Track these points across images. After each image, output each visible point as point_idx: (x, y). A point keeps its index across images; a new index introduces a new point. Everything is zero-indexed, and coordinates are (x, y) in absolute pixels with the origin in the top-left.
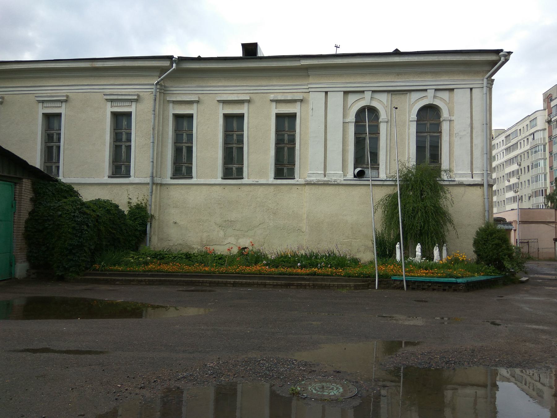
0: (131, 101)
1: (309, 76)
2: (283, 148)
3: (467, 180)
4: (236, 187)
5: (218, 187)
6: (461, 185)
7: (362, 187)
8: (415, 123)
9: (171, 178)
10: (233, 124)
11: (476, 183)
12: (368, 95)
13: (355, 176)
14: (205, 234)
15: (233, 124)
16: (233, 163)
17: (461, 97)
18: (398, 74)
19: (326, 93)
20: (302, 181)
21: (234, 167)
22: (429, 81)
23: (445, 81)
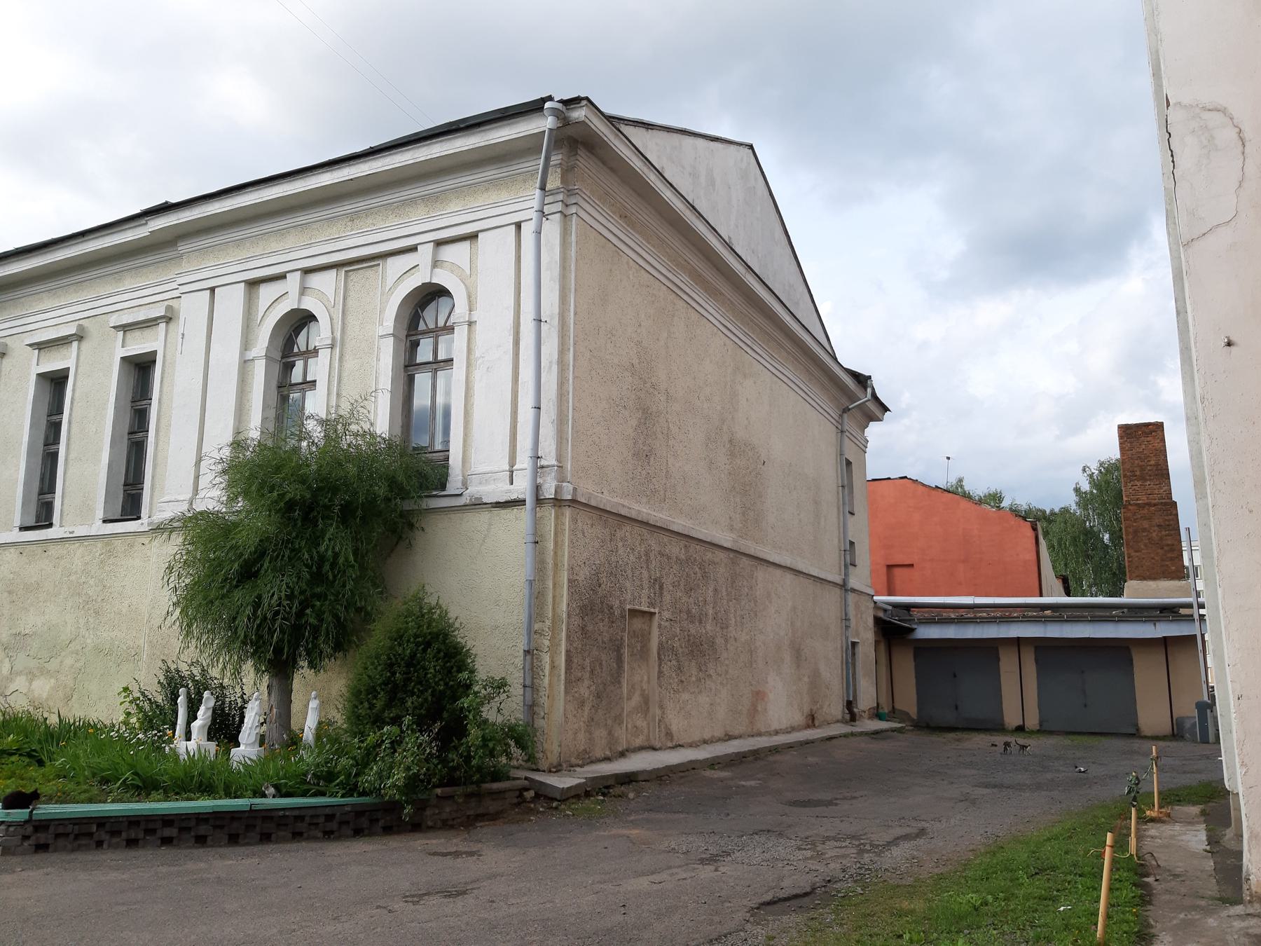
1: (181, 256)
4: (38, 549)
6: (478, 505)
12: (294, 281)
17: (496, 250)
18: (353, 217)
19: (212, 290)
22: (419, 223)
23: (453, 215)
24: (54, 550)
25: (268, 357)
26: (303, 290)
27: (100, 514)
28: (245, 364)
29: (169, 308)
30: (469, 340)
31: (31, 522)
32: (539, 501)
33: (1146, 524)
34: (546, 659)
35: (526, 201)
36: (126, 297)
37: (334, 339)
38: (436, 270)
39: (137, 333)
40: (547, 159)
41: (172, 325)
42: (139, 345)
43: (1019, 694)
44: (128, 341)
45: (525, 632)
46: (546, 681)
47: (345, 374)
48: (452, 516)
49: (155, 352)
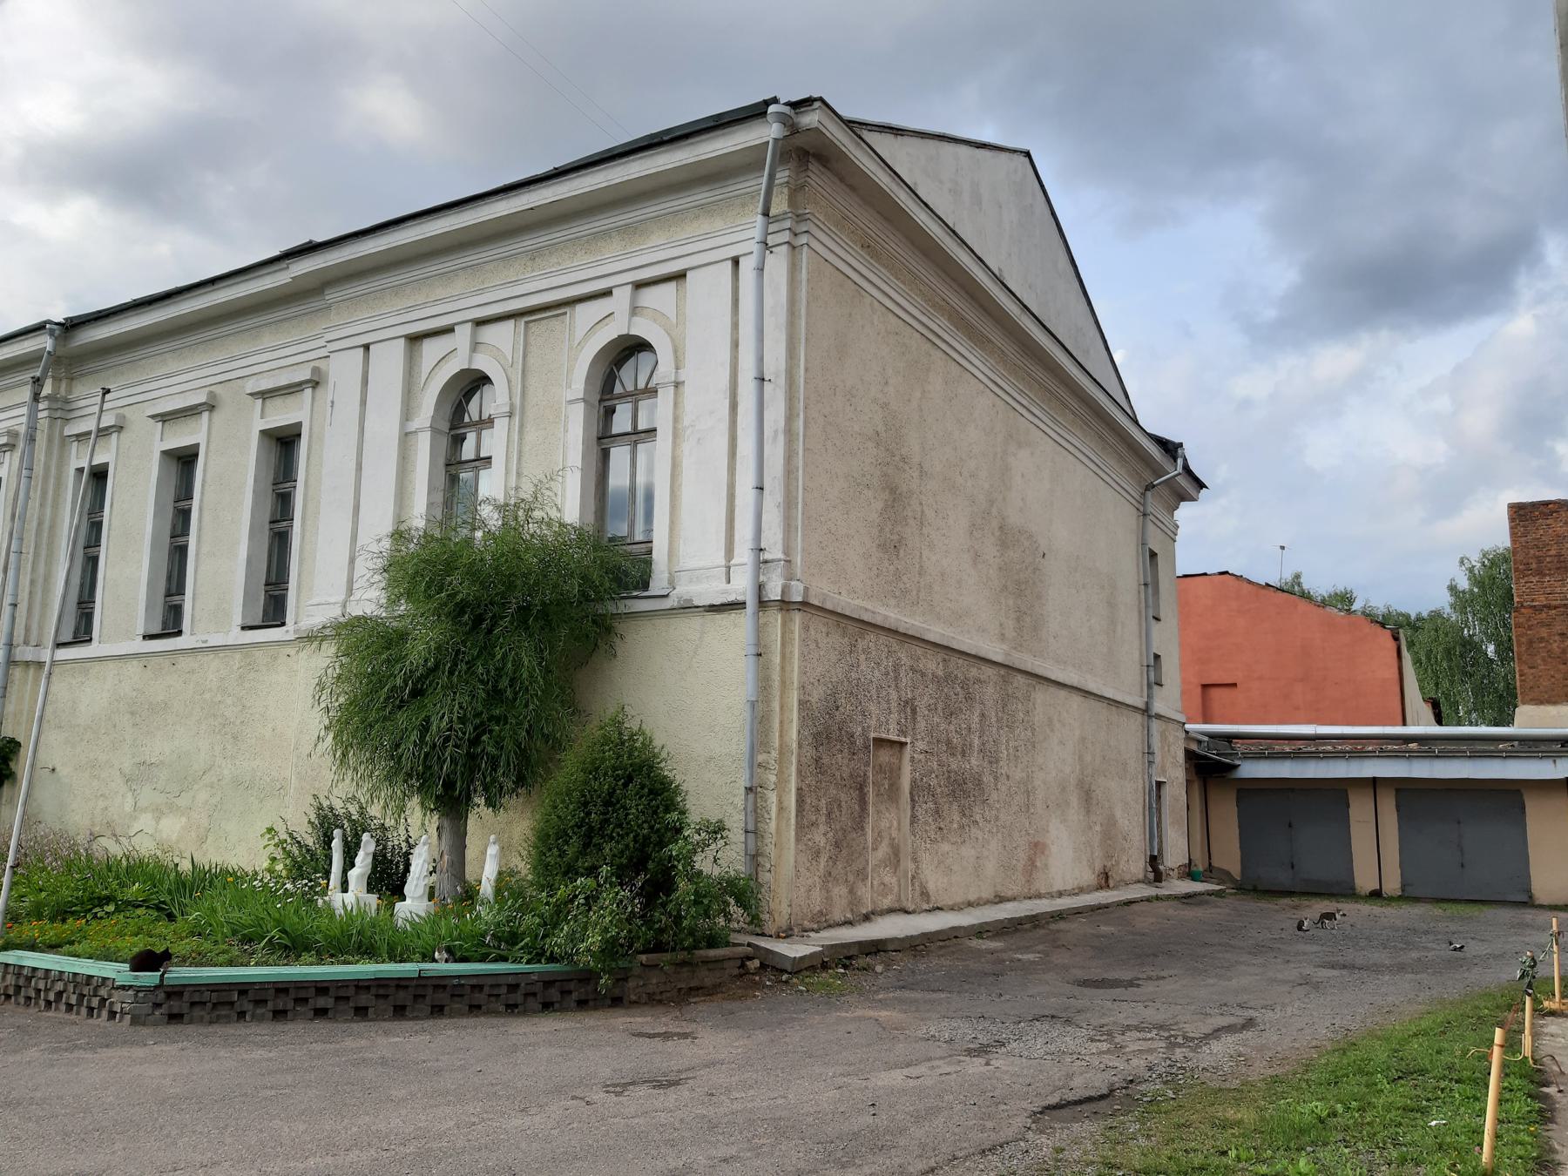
1: (329, 307)
3: (713, 591)
6: (687, 608)
8: (581, 405)
12: (463, 335)
14: (101, 804)
18: (534, 255)
19: (367, 347)
22: (612, 260)
23: (656, 250)
24: (185, 663)
25: (434, 430)
26: (475, 346)
27: (238, 620)
28: (406, 437)
29: (316, 370)
30: (676, 404)
31: (157, 629)
32: (762, 604)
33: (1544, 632)
34: (773, 797)
35: (744, 232)
37: (512, 405)
38: (636, 319)
39: (278, 402)
40: (772, 177)
41: (320, 391)
42: (281, 415)
43: (1374, 848)
44: (267, 410)
45: (745, 765)
46: (773, 825)
47: (526, 449)
48: (657, 622)
49: (299, 425)
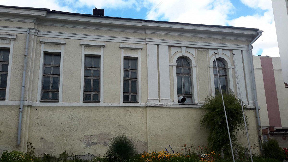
0: (10, 39)
2: (128, 81)
4: (94, 109)
5: (80, 109)
7: (185, 109)
9: (40, 101)
10: (93, 62)
11: (251, 108)
13: (179, 102)
15: (93, 62)
16: (92, 91)
20: (143, 105)
21: (92, 94)
23: (227, 45)
24: (100, 110)
36: (124, 39)
